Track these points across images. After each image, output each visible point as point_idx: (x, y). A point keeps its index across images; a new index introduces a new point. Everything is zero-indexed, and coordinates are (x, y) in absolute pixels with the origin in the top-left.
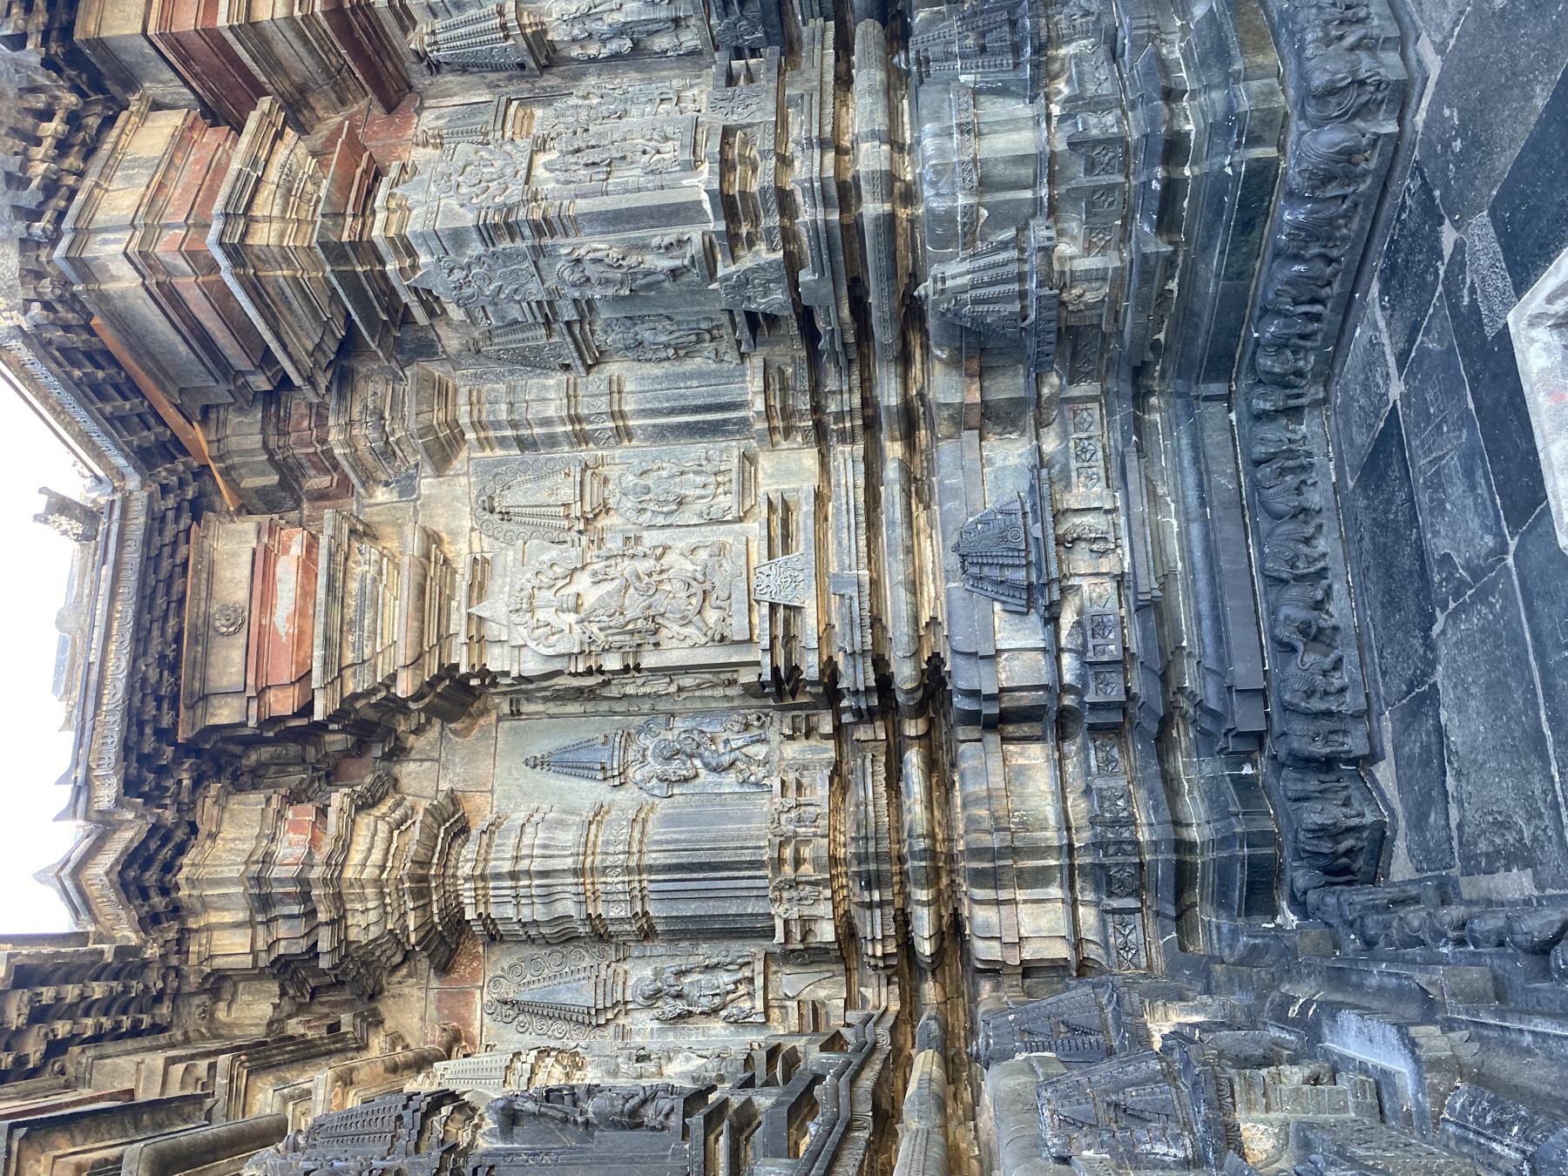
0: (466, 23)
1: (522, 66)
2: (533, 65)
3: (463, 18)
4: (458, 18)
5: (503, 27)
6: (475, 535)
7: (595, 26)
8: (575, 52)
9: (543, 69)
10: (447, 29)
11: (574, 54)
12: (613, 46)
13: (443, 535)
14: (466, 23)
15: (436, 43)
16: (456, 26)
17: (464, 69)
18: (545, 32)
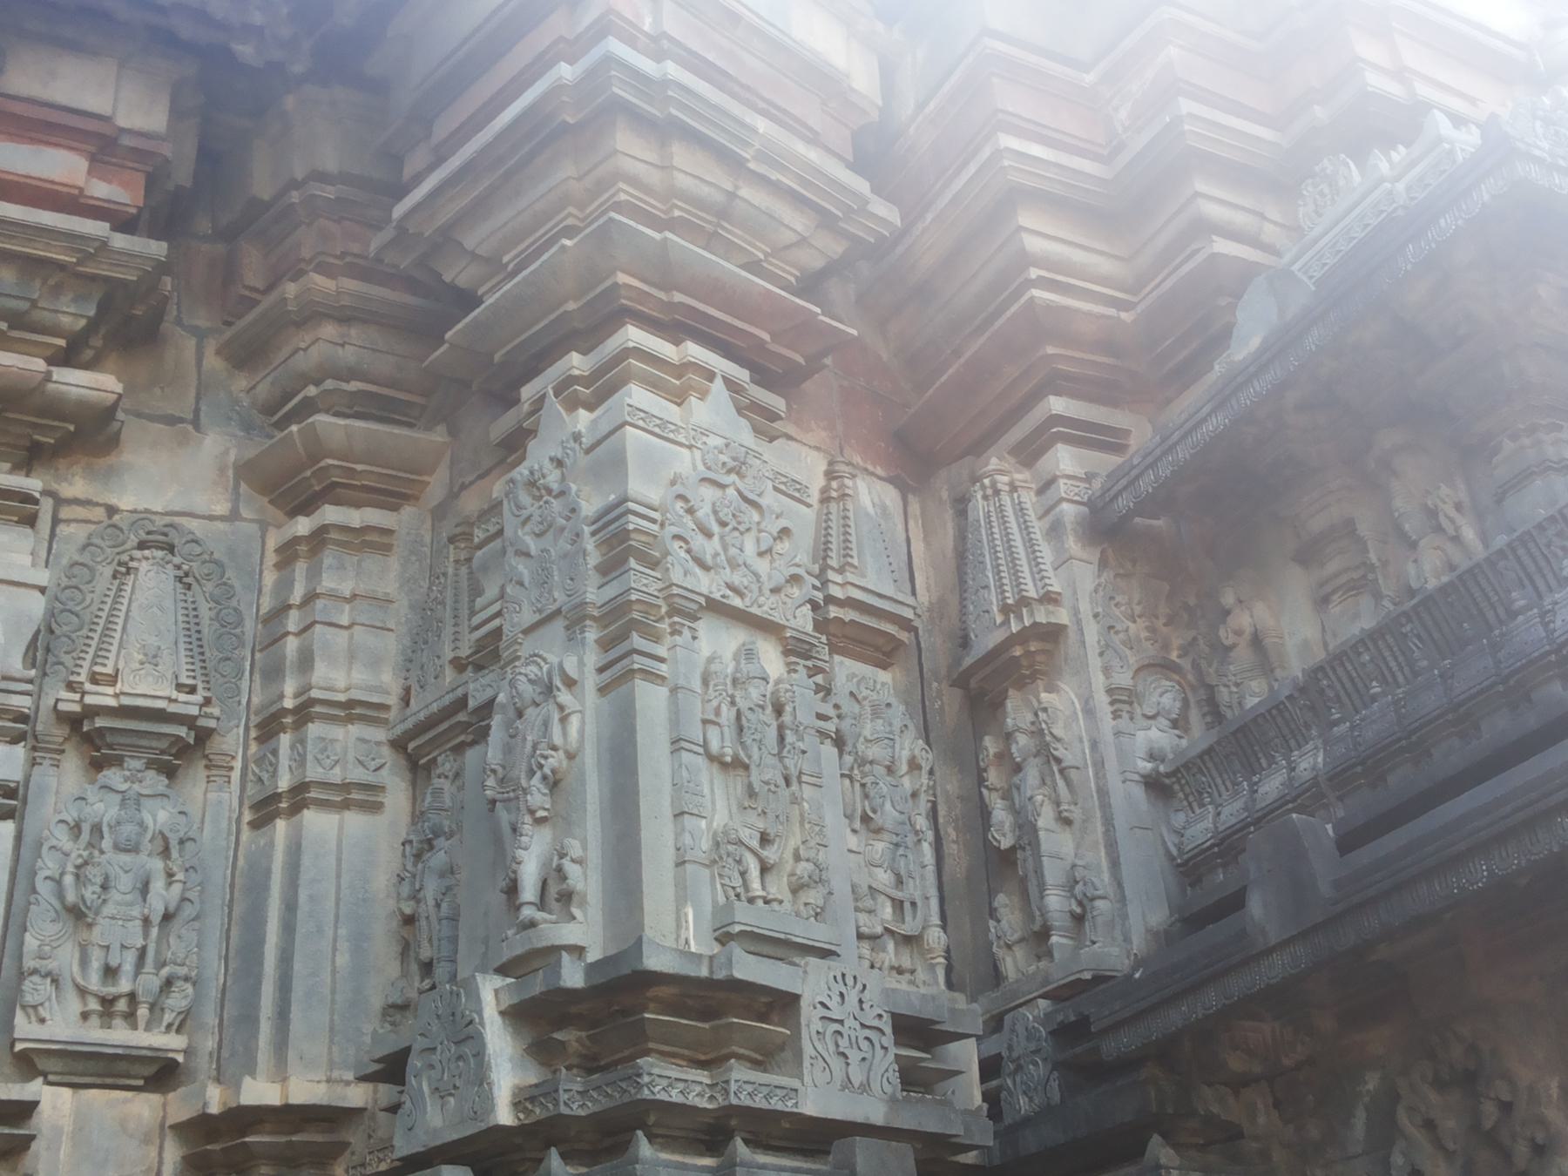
0: (1030, 544)
1: (965, 643)
2: (968, 661)
3: (1038, 535)
4: (1038, 529)
5: (1024, 601)
6: (99, 513)
7: (1032, 774)
8: (991, 745)
9: (961, 681)
10: (1020, 510)
11: (988, 742)
12: (1000, 813)
13: (112, 459)
14: (1030, 544)
15: (997, 492)
16: (1025, 527)
17: (961, 555)
18: (1021, 684)
